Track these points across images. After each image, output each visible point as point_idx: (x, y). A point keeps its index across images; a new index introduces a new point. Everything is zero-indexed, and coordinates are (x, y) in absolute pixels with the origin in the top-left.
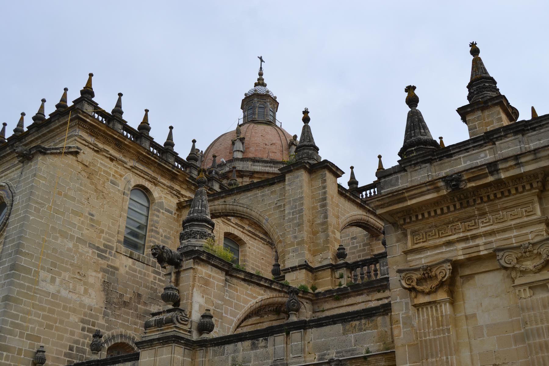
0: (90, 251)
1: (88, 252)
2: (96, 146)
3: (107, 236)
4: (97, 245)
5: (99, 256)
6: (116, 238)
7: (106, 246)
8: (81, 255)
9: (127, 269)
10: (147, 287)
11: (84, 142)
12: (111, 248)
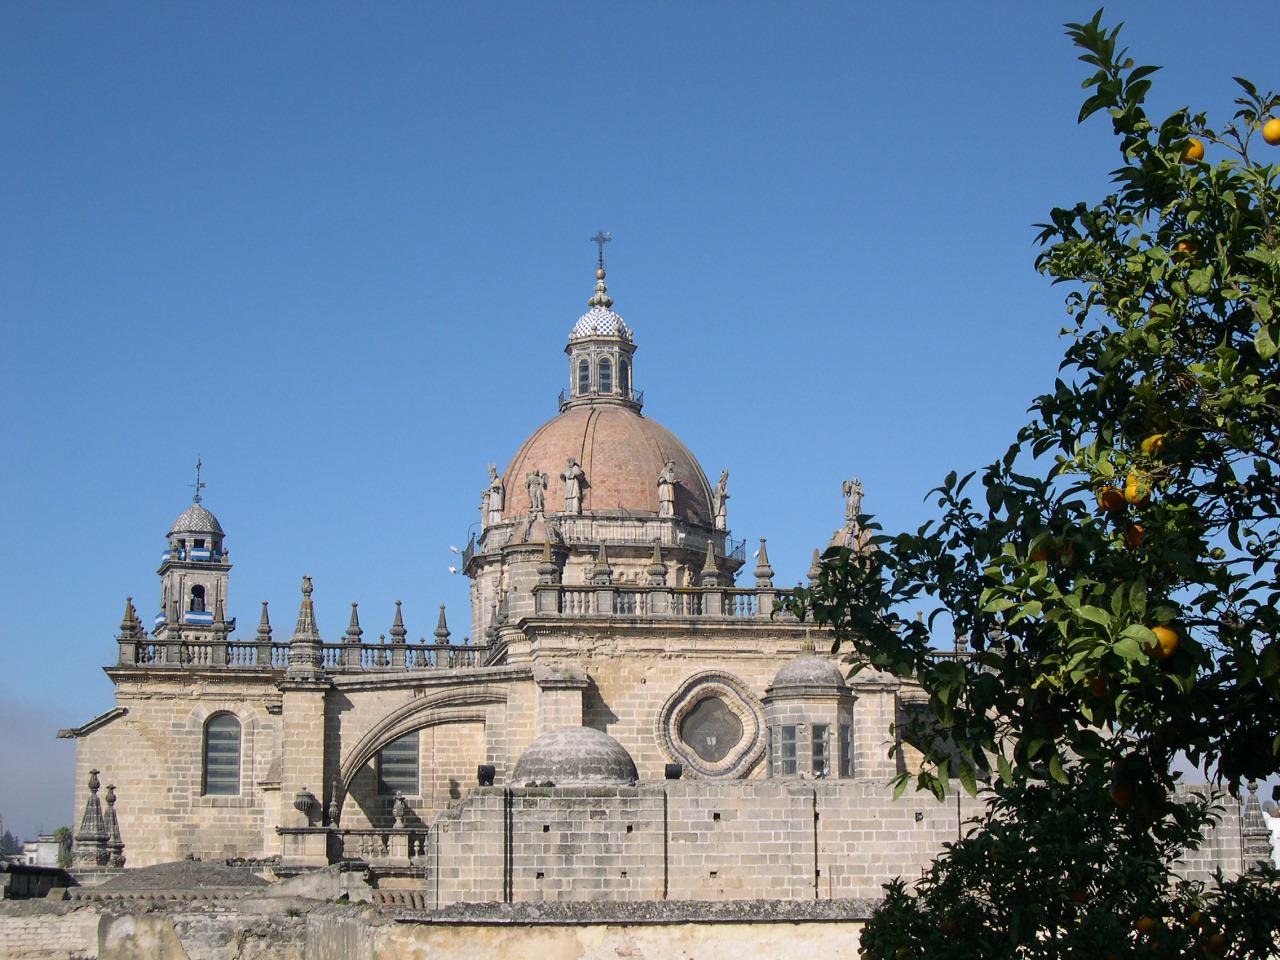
0: (158, 817)
1: (155, 819)
2: (143, 693)
3: (178, 793)
4: (165, 808)
5: (170, 819)
6: (190, 791)
7: (176, 805)
8: (147, 825)
9: (212, 822)
10: (241, 833)
11: (128, 696)
12: (187, 805)
